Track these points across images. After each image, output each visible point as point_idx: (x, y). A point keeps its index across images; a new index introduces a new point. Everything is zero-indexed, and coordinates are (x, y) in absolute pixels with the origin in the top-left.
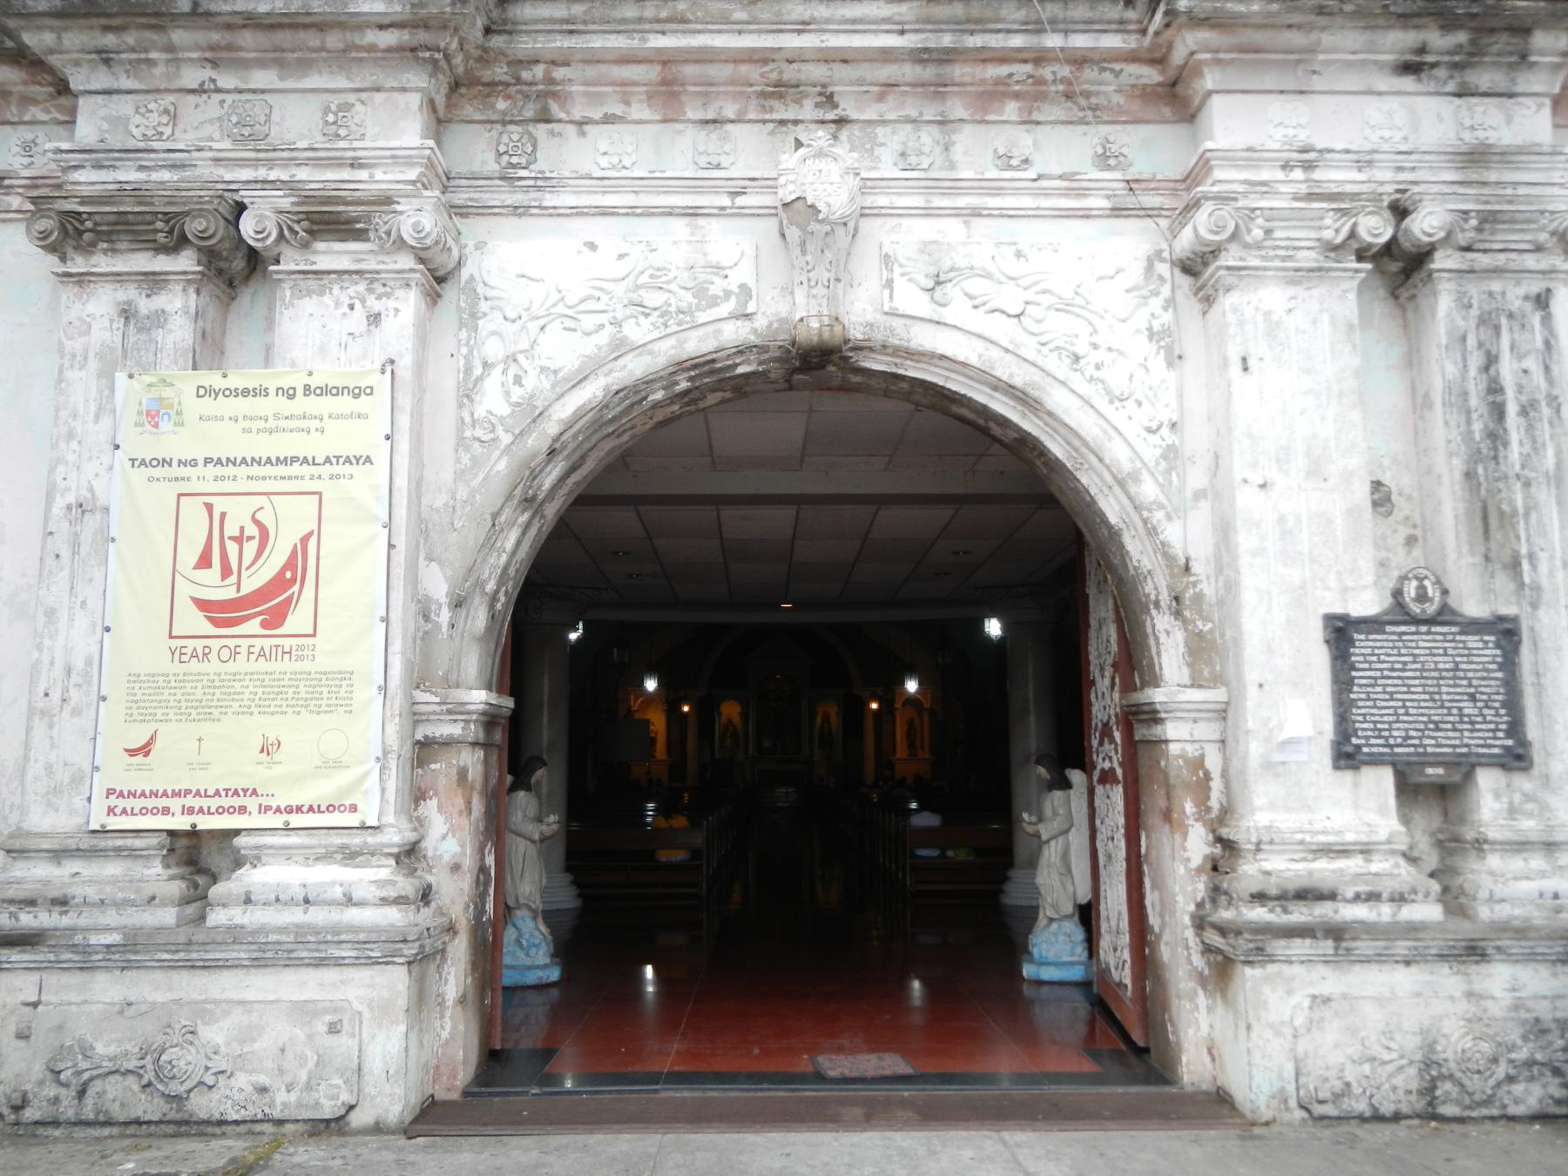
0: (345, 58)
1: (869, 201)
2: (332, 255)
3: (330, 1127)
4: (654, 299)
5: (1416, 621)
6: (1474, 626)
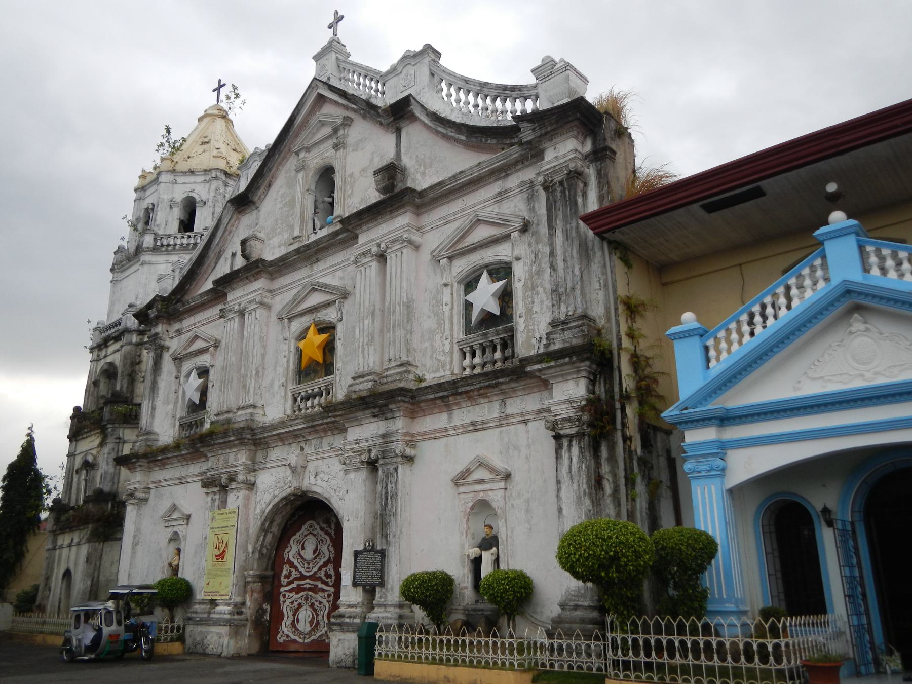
0: (234, 446)
1: (308, 458)
2: (234, 485)
3: (219, 656)
4: (278, 485)
5: (368, 551)
6: (377, 552)
